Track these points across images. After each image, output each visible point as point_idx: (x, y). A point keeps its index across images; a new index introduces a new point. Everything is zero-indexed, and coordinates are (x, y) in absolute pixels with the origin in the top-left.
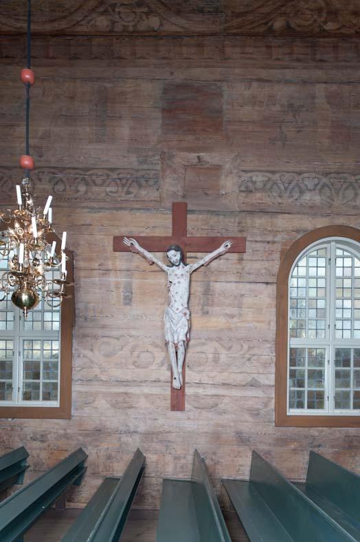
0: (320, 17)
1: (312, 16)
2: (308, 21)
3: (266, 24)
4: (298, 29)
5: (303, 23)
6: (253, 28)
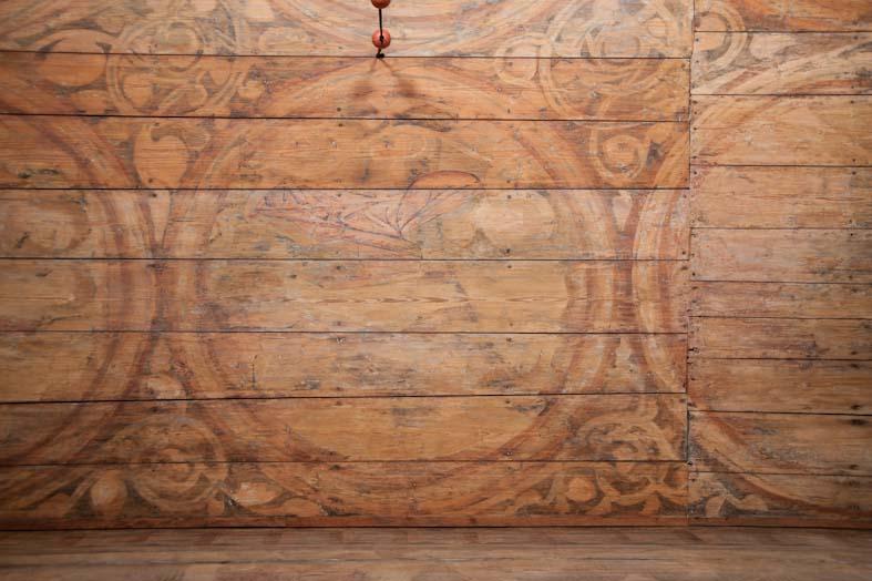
0: (211, 464)
1: (191, 464)
2: (184, 480)
3: (69, 491)
4: (164, 505)
5: (172, 485)
6: (35, 505)
